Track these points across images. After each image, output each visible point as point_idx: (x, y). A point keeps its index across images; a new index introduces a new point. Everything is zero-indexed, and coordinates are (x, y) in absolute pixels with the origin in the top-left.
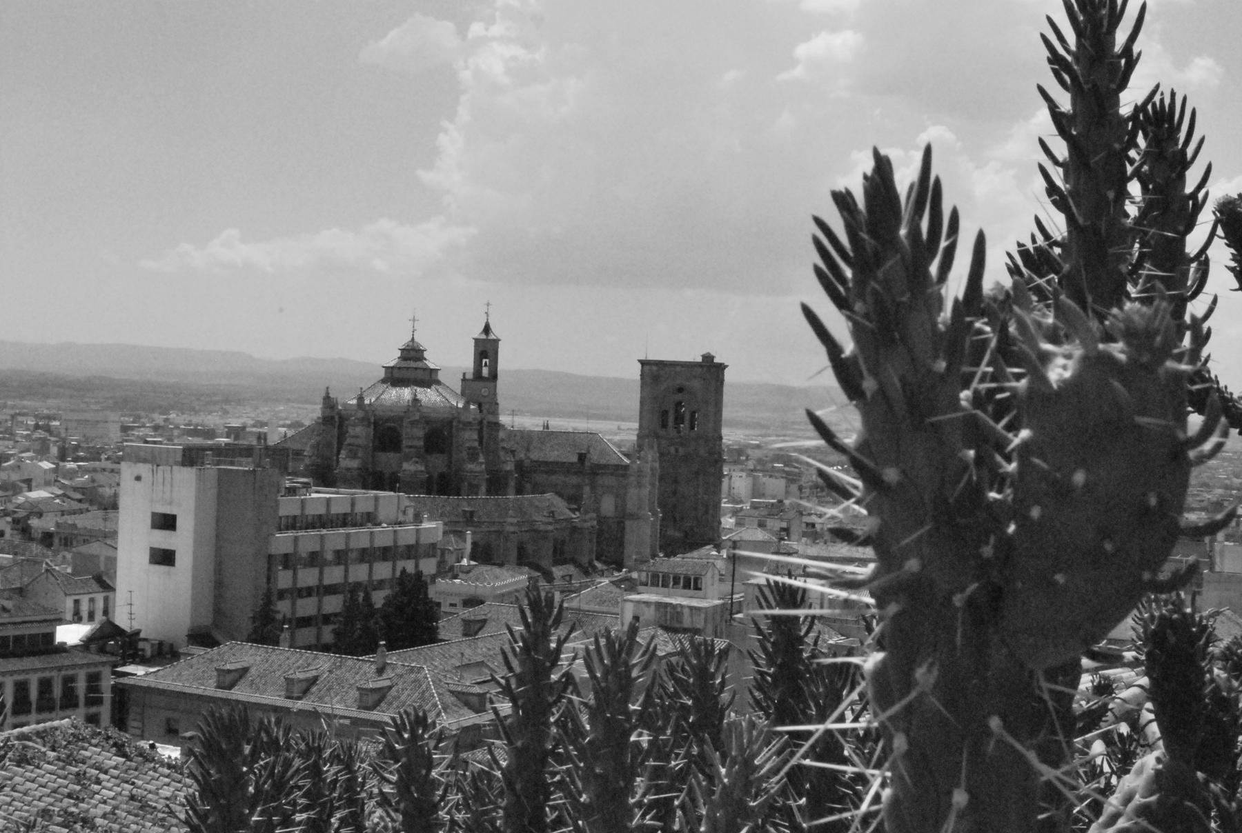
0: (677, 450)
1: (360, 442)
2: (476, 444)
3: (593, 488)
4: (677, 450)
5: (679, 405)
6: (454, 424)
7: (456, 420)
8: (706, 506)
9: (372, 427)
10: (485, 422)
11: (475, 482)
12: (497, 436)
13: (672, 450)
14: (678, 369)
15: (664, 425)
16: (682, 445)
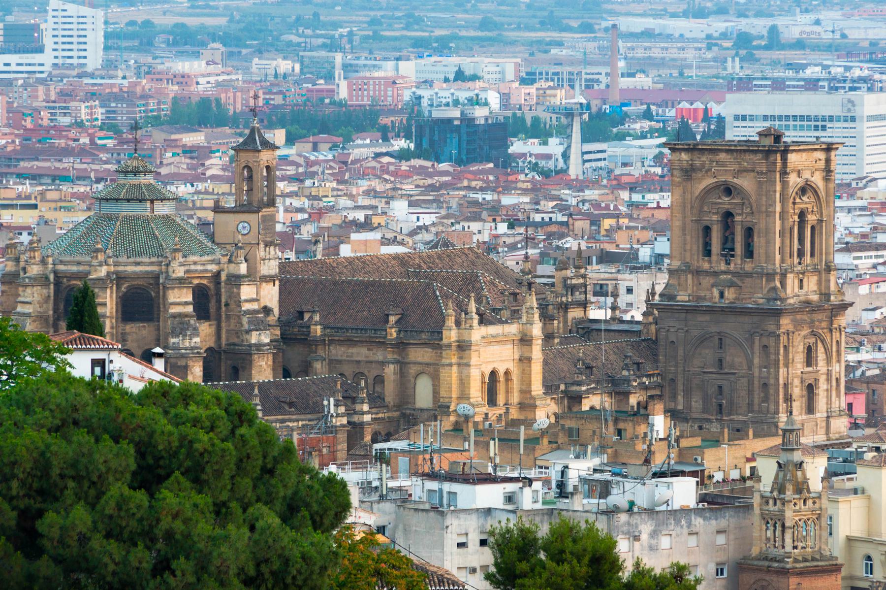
0: (722, 295)
1: (28, 309)
2: (190, 309)
3: (402, 365)
4: (722, 295)
5: (728, 215)
6: (161, 281)
7: (164, 275)
8: (765, 385)
9: (52, 287)
10: (223, 277)
11: (182, 363)
12: (239, 294)
13: (716, 292)
14: (722, 156)
15: (708, 253)
16: (732, 285)
